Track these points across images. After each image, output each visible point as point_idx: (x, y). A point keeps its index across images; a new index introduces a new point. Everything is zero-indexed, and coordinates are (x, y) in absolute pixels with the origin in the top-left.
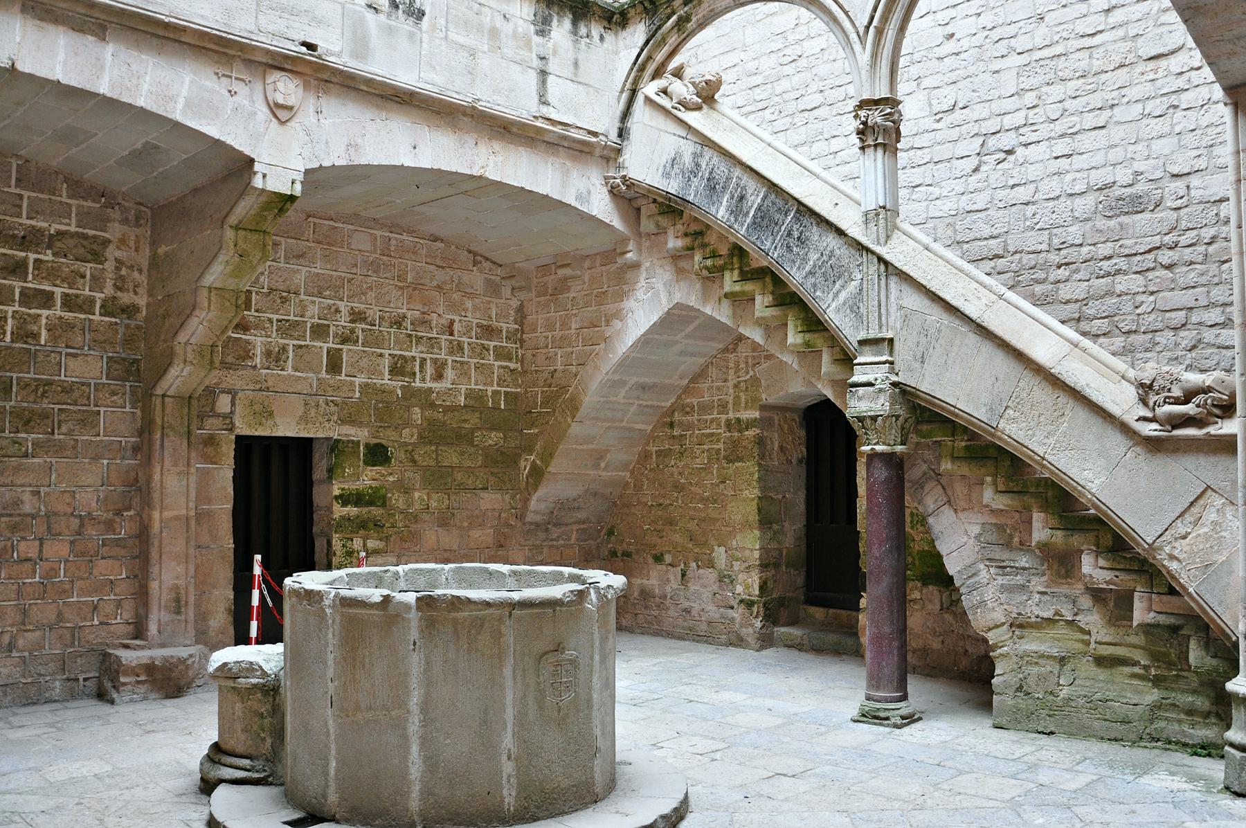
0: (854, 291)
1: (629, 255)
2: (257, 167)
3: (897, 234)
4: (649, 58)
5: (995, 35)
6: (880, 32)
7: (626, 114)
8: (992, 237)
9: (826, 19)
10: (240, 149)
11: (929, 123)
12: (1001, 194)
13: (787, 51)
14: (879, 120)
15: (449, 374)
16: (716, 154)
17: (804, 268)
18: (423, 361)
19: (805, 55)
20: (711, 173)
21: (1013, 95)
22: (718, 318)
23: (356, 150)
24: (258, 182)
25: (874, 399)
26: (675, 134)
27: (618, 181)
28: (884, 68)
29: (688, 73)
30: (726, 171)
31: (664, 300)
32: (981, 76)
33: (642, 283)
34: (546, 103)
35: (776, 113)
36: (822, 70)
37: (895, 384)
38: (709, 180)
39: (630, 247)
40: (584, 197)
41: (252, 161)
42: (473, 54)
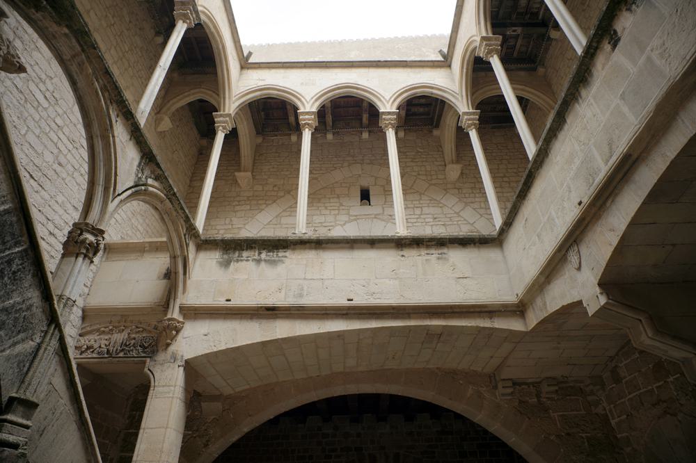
17: (4, 302)
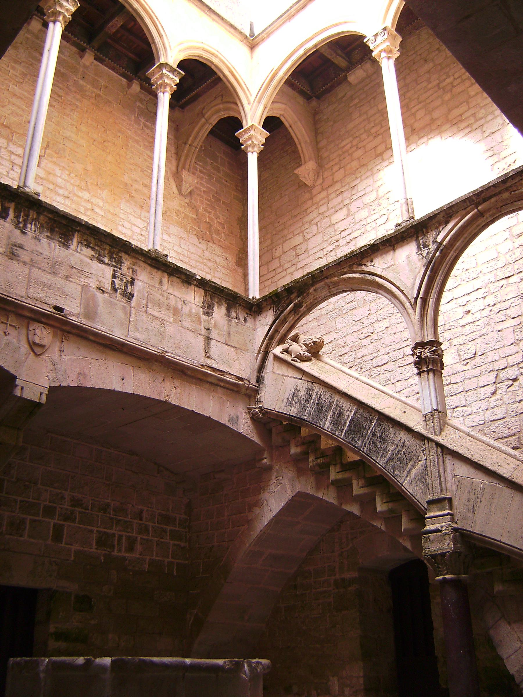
0: (421, 468)
1: (265, 461)
2: (18, 382)
3: (447, 428)
4: (276, 331)
5: (496, 309)
6: (425, 301)
7: (262, 367)
8: (510, 436)
9: (389, 297)
10: (8, 369)
11: (460, 367)
12: (513, 407)
13: (364, 331)
14: (428, 354)
15: (138, 547)
16: (321, 387)
18: (120, 537)
19: (375, 332)
20: (319, 400)
21: (512, 344)
22: (327, 499)
23: (84, 378)
24: (18, 392)
25: (441, 541)
26: (294, 378)
27: (257, 410)
28: (429, 323)
29: (302, 338)
30: (329, 398)
31: (289, 490)
32: (491, 334)
33: (274, 480)
34: (209, 357)
35: (359, 370)
36: (387, 340)
37: (455, 530)
38: (317, 404)
39: (265, 456)
40: (235, 420)
41: (14, 378)
42: (163, 322)
